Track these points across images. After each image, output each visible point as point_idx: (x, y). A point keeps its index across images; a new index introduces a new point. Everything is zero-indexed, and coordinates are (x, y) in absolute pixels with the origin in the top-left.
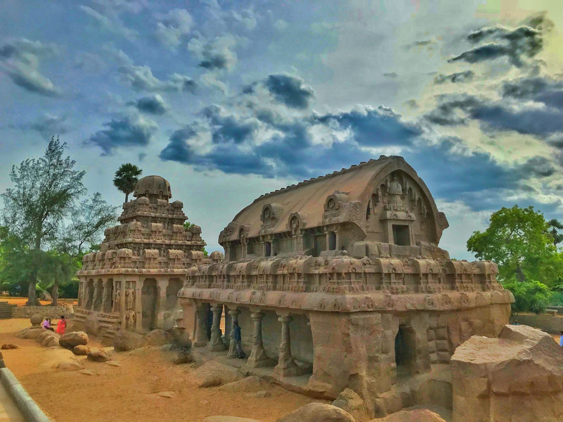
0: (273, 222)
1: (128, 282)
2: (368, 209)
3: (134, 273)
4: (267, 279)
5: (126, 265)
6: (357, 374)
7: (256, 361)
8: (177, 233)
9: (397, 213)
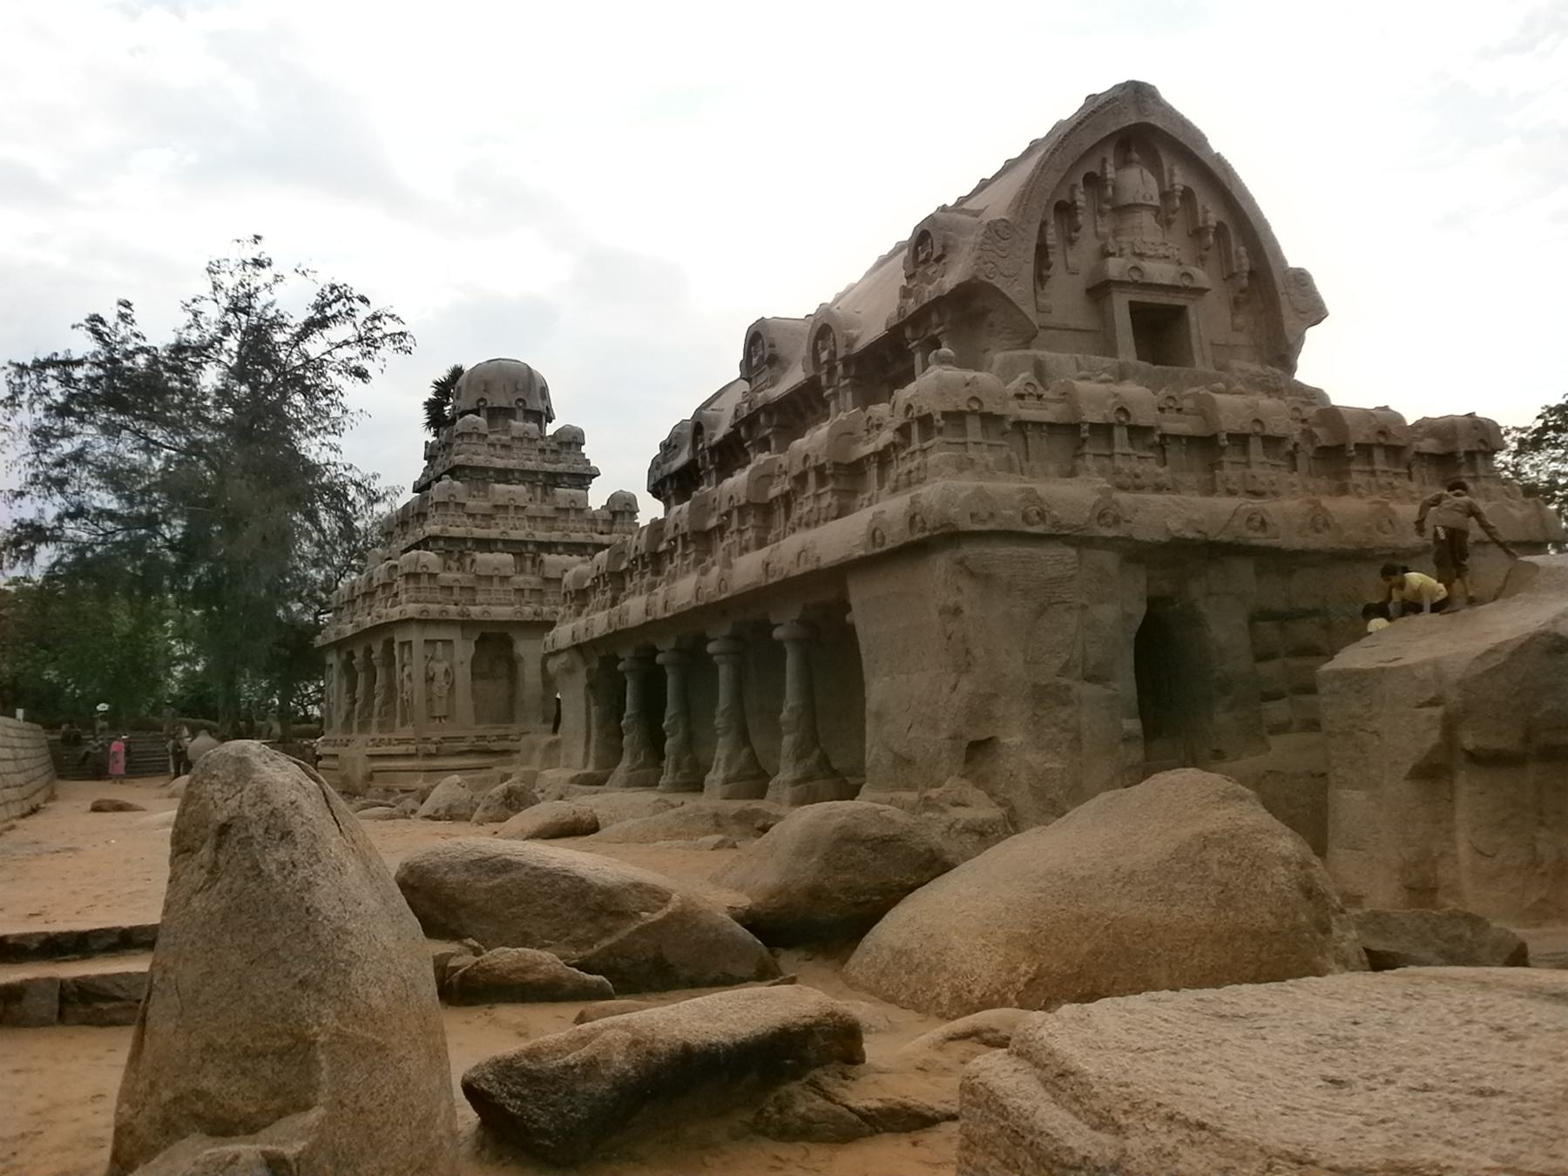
2: (1042, 250)
3: (444, 616)
4: (742, 521)
5: (422, 596)
6: (990, 740)
7: (726, 781)
8: (567, 510)
9: (1147, 265)
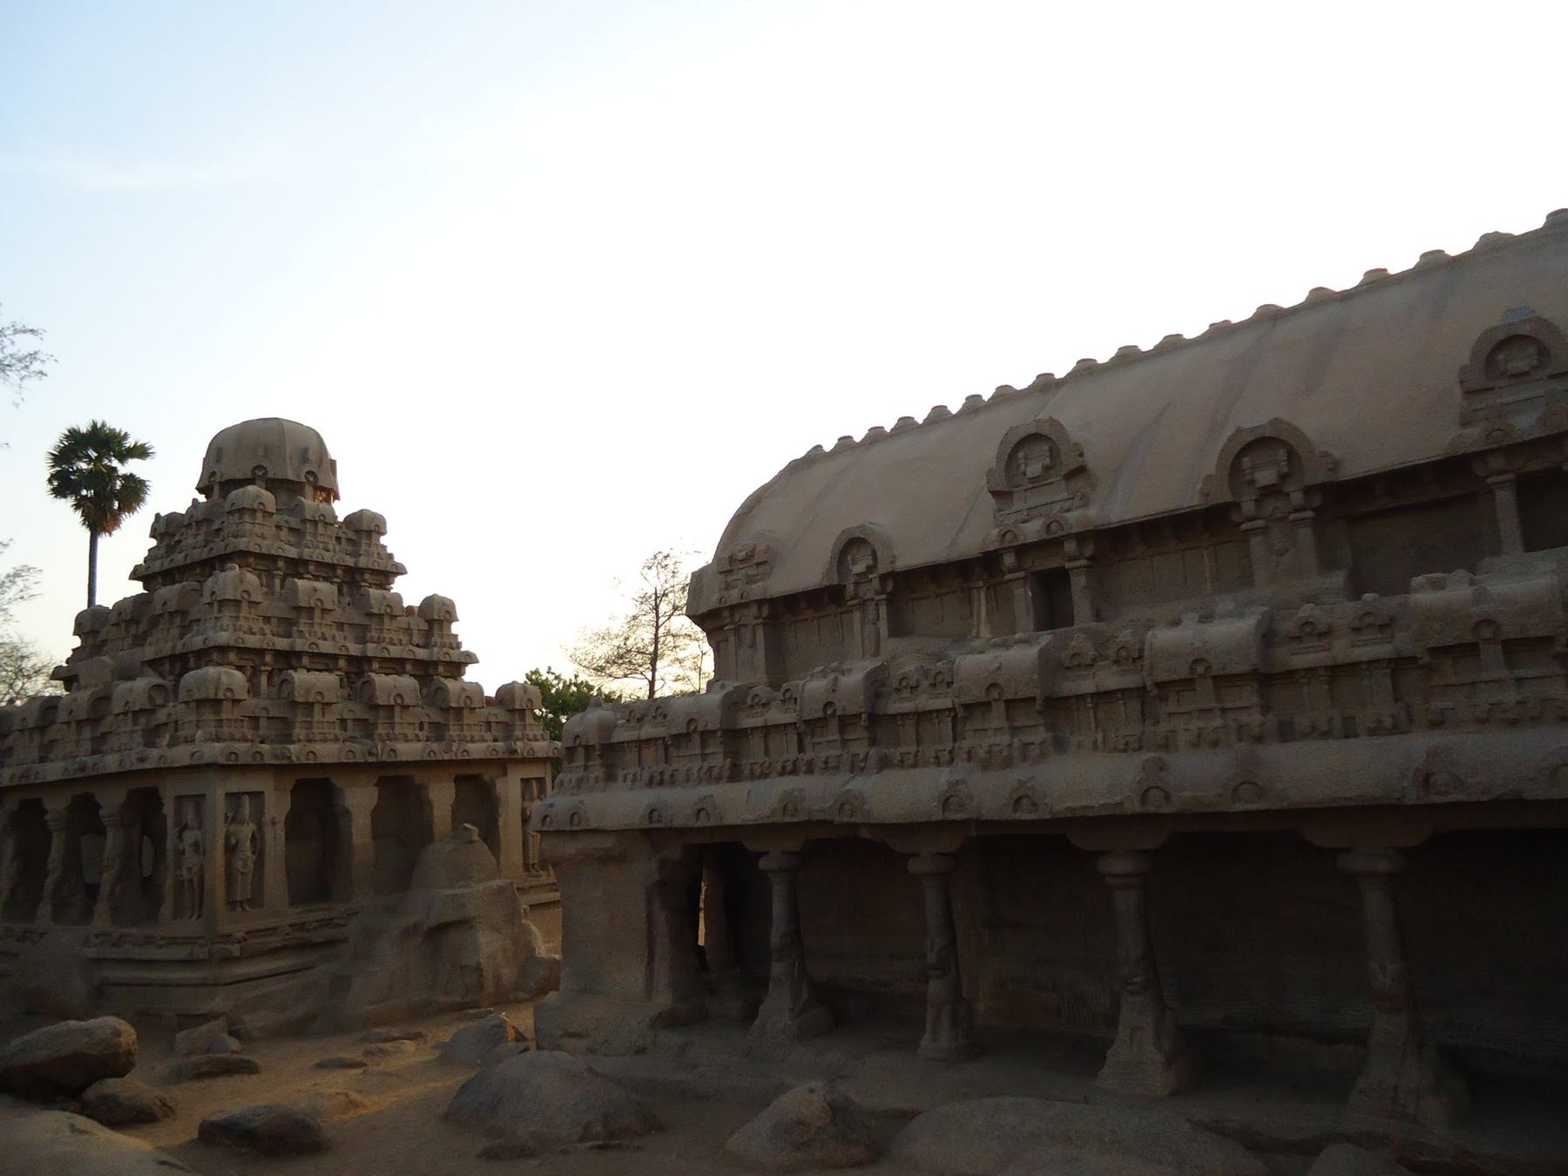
0: (1079, 484)
1: (234, 797)
